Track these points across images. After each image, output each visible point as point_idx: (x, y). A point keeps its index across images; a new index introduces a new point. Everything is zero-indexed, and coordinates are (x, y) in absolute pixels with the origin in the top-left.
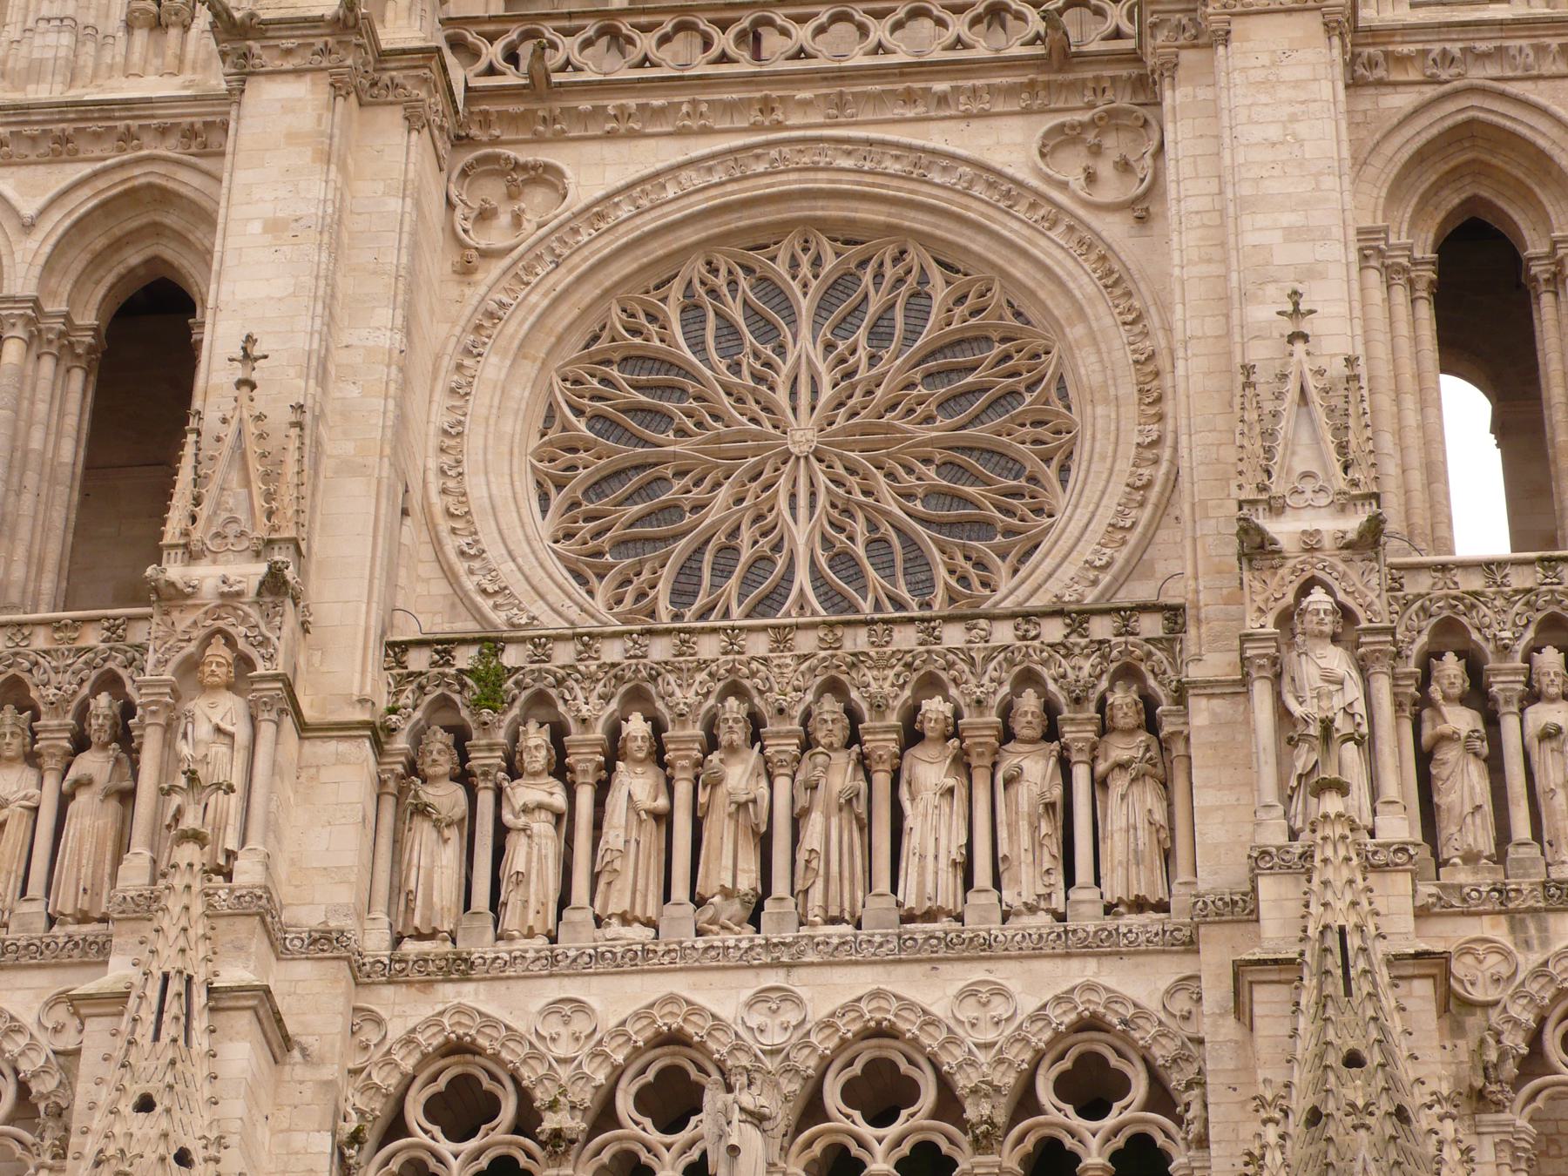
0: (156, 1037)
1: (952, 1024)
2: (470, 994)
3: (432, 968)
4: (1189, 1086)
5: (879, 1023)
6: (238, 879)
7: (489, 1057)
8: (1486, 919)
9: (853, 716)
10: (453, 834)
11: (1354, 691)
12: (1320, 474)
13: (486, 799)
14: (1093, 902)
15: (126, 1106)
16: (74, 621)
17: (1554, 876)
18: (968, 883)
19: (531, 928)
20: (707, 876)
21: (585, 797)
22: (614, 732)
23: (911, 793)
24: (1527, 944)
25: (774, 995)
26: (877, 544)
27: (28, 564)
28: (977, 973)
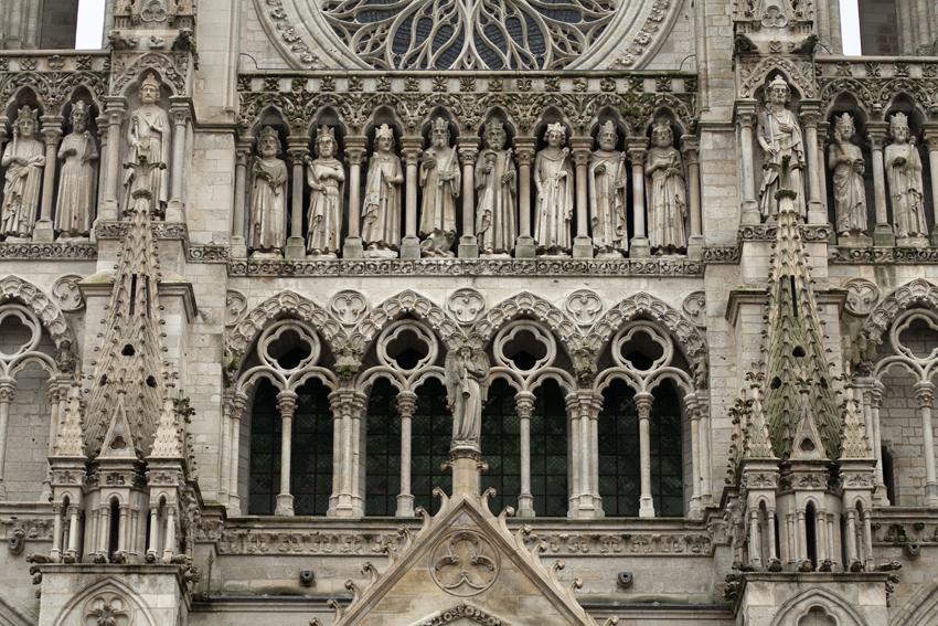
0: (132, 313)
1: (567, 314)
2: (293, 285)
3: (271, 269)
4: (697, 353)
5: (525, 311)
6: (168, 219)
7: (304, 321)
8: (862, 267)
9: (508, 130)
10: (279, 190)
11: (798, 138)
12: (780, 7)
13: (298, 170)
14: (645, 247)
15: (118, 351)
16: (61, 55)
17: (899, 245)
18: (574, 233)
19: (327, 248)
20: (426, 222)
21: (355, 172)
22: (371, 134)
23: (541, 177)
24: (884, 283)
25: (467, 293)
26: (513, 22)
27: (21, 12)
28: (580, 285)
